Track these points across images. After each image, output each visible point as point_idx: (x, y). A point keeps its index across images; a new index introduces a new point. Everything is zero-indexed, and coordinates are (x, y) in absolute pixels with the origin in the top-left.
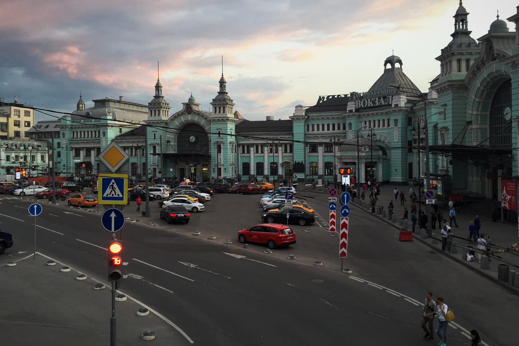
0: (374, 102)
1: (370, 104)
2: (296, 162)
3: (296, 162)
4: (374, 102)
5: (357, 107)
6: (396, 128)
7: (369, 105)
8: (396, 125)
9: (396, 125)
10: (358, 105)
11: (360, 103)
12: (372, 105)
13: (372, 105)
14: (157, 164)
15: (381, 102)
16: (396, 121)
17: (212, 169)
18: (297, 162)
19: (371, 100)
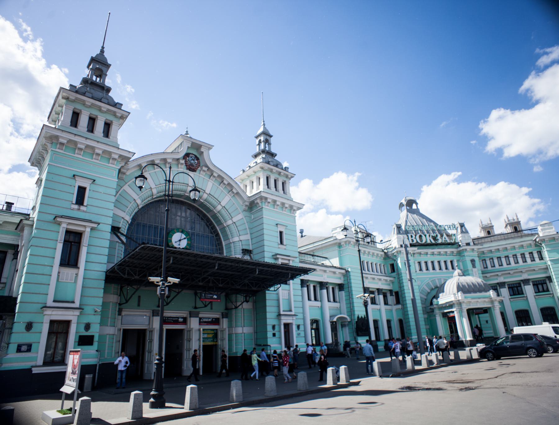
0: (435, 238)
1: (429, 240)
2: (358, 317)
3: (358, 317)
4: (435, 238)
5: (411, 242)
6: (474, 270)
7: (429, 242)
8: (474, 266)
9: (474, 266)
10: (412, 240)
11: (415, 238)
12: (433, 242)
13: (433, 242)
14: (77, 305)
15: (445, 238)
16: (473, 261)
17: (269, 328)
18: (360, 317)
19: (429, 236)
